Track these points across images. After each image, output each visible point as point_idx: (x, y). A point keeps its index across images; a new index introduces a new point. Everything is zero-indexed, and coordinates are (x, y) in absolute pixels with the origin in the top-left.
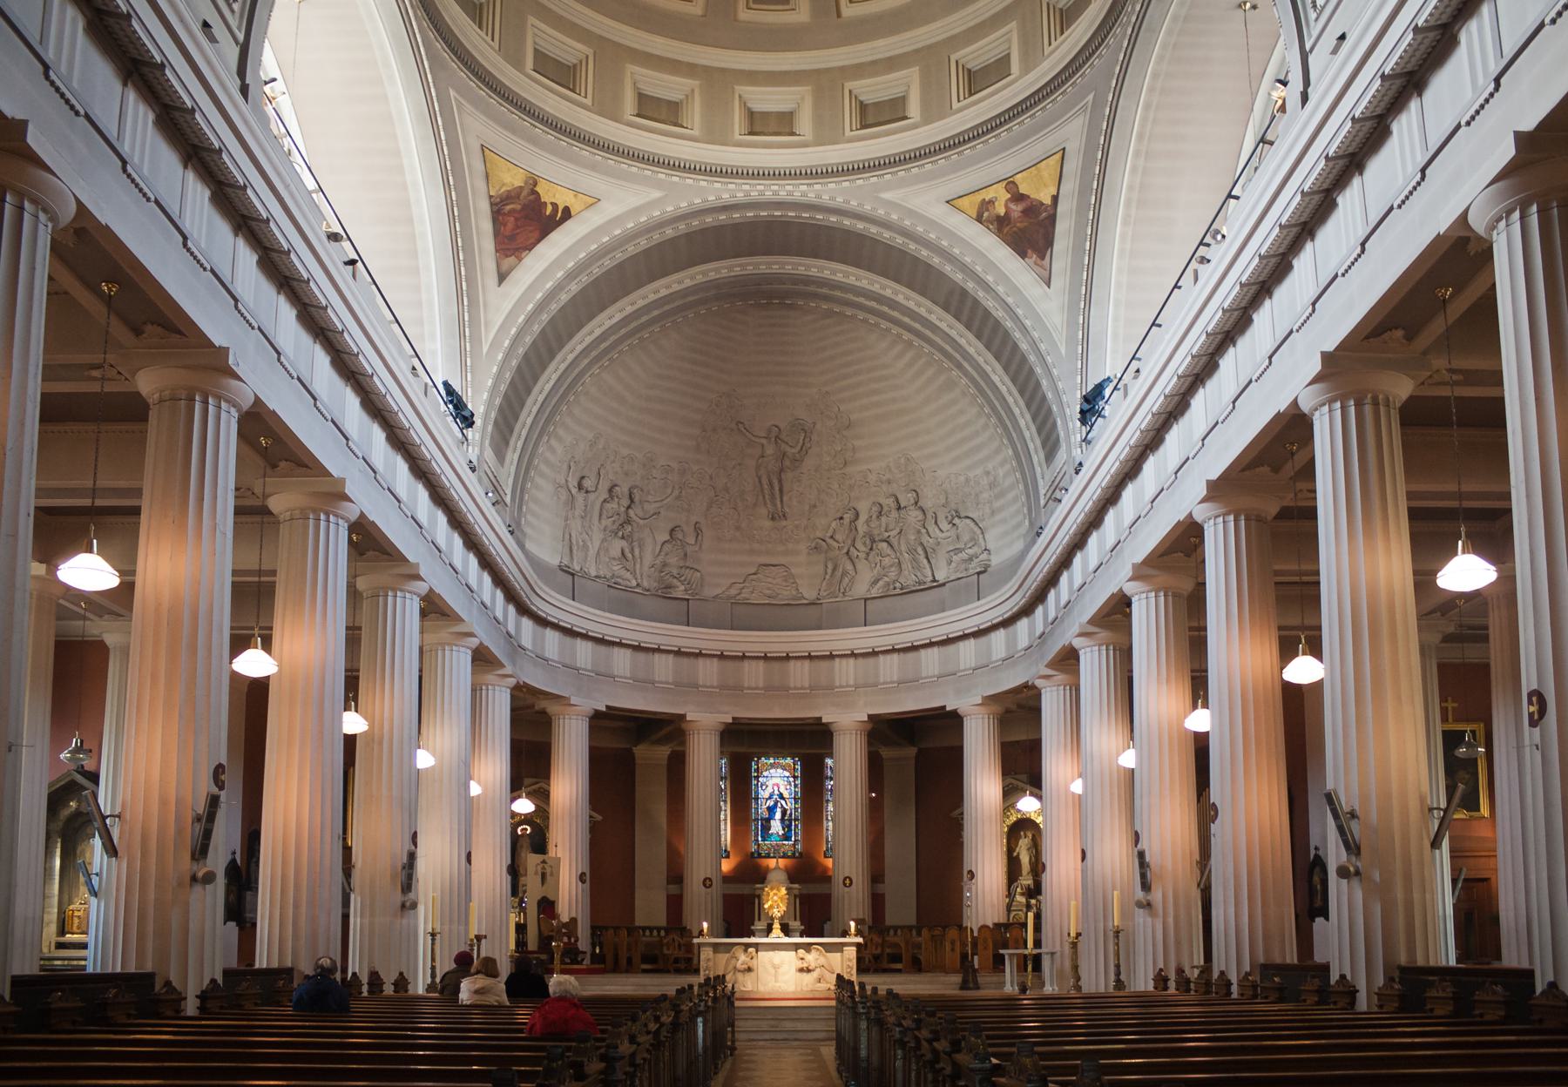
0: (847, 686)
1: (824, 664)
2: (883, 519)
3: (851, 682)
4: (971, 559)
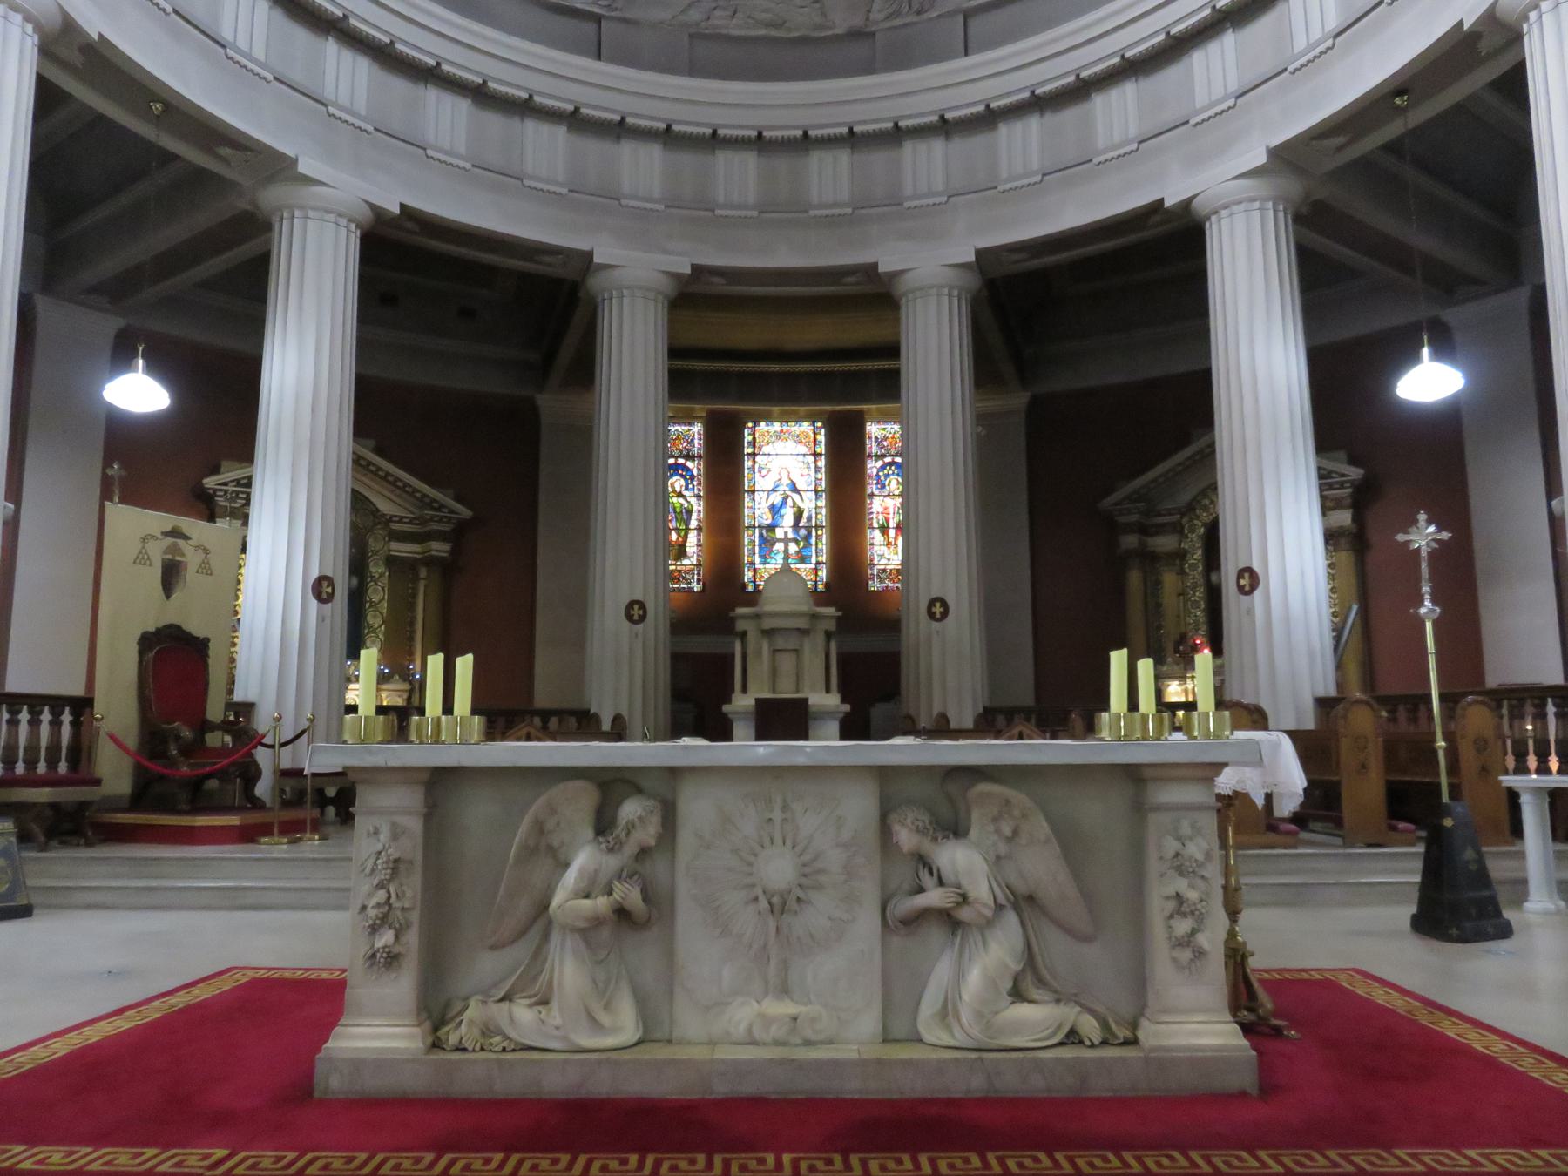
0: (931, 194)
1: (878, 159)
3: (939, 185)
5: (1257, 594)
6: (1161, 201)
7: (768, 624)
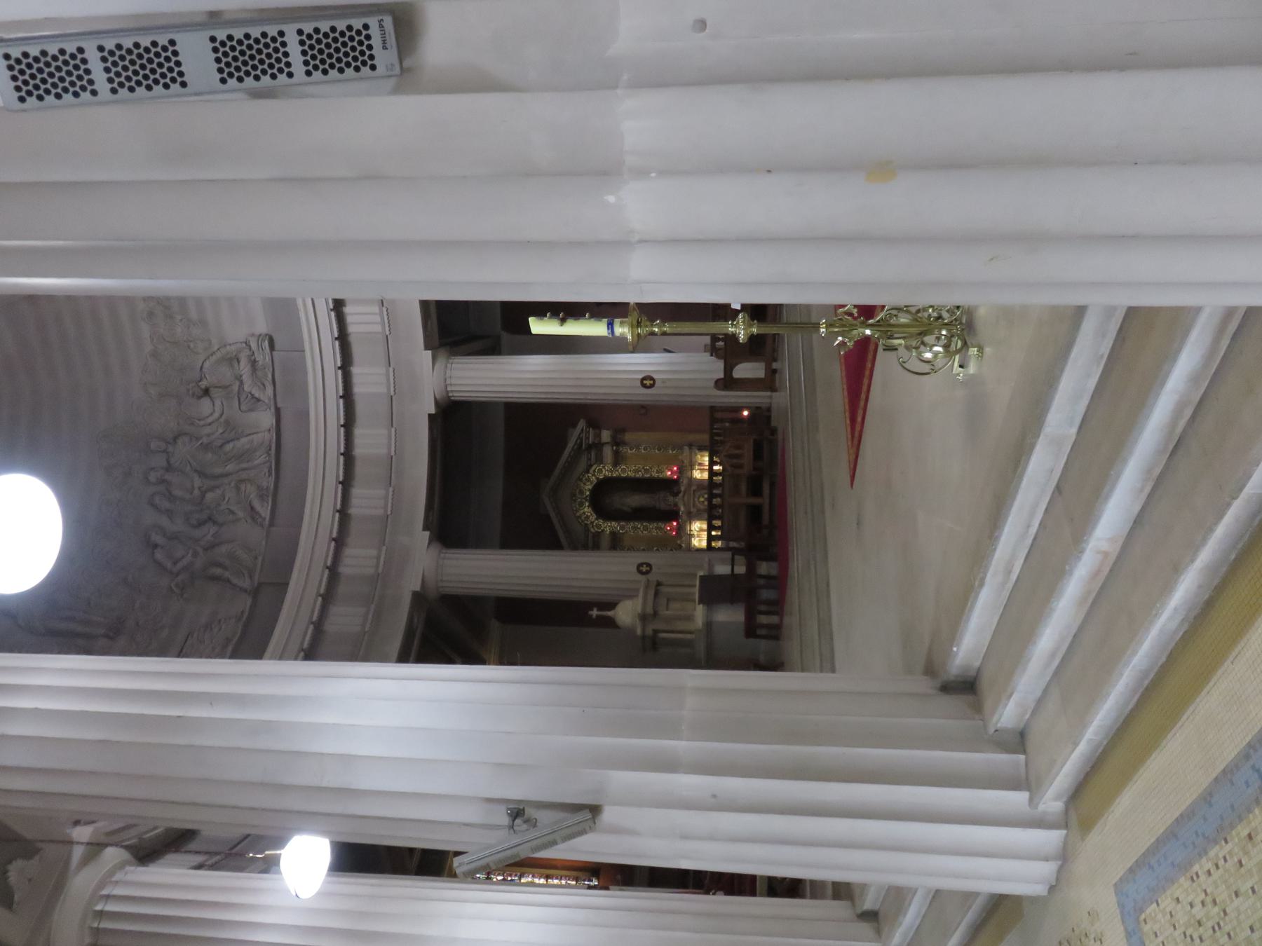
0: (378, 558)
2: (177, 492)
4: (254, 363)
5: (655, 376)
6: (430, 415)
7: (649, 610)
